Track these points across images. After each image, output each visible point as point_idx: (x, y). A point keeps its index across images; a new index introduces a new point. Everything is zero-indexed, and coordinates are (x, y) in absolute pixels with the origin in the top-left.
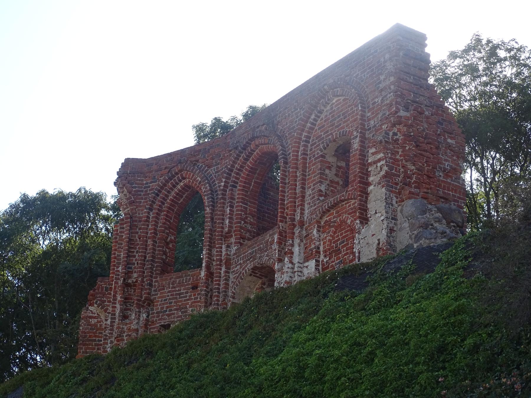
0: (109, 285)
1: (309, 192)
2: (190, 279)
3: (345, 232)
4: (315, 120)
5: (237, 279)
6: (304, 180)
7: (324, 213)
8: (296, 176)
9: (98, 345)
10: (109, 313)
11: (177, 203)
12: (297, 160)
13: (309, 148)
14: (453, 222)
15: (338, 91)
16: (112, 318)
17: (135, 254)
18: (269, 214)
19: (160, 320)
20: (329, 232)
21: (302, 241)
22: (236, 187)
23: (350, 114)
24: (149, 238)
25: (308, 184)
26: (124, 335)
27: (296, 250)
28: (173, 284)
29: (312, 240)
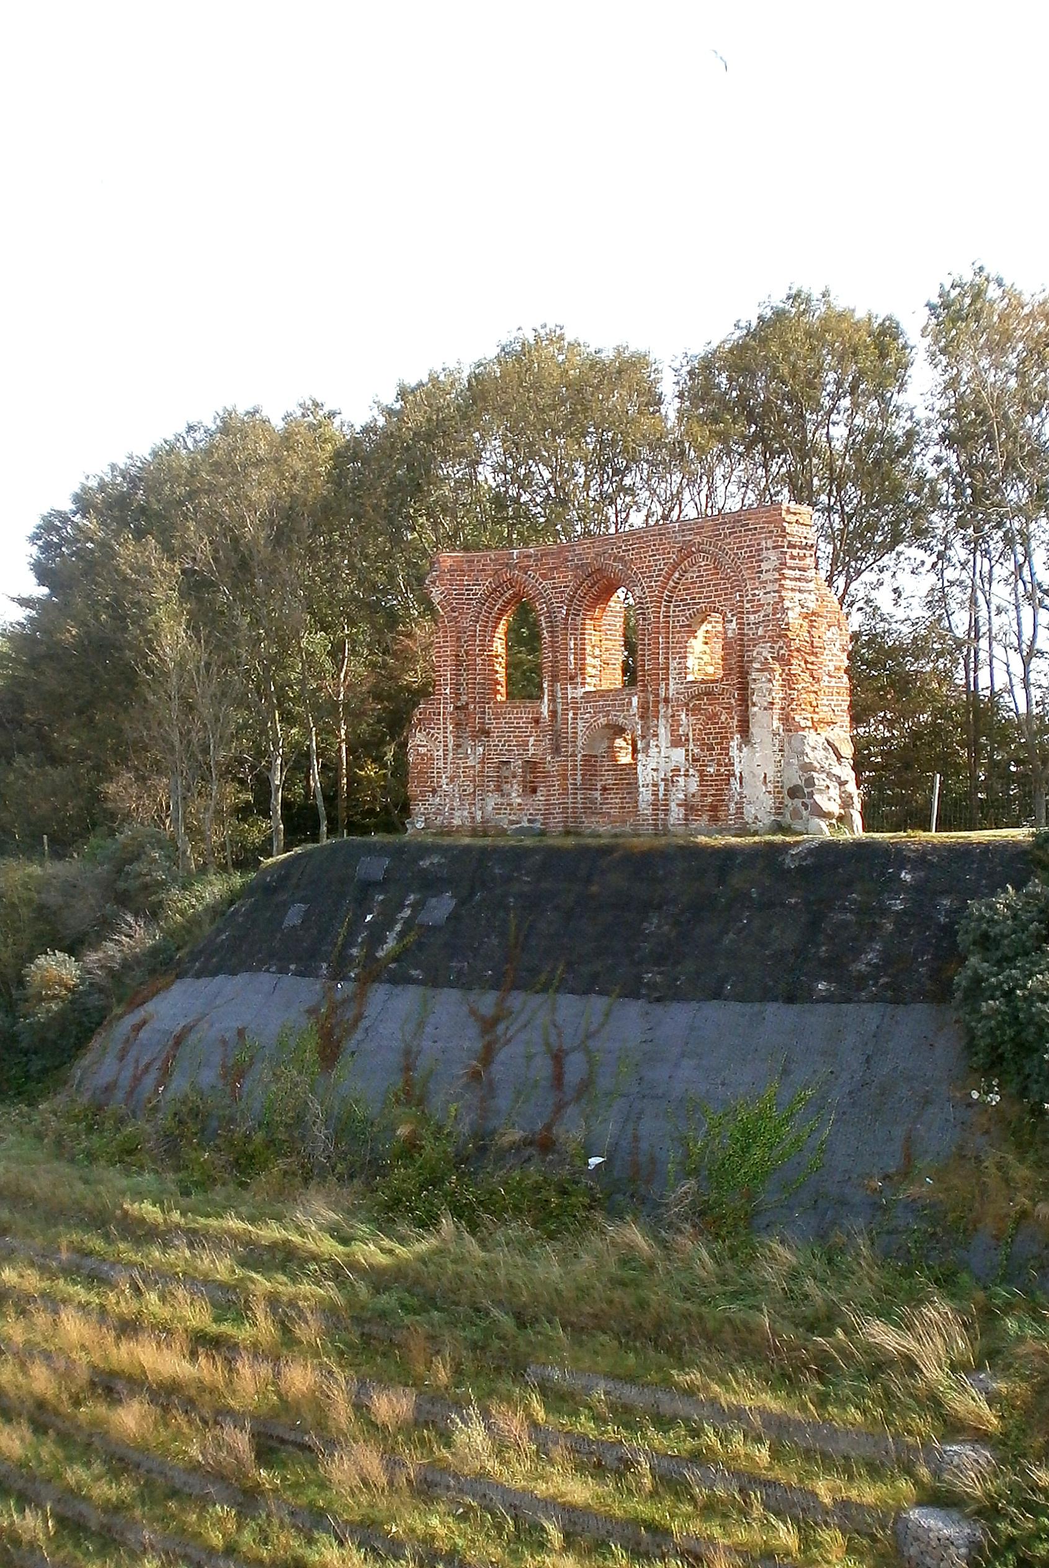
1: (673, 664)
12: (658, 622)
23: (722, 590)
27: (662, 731)
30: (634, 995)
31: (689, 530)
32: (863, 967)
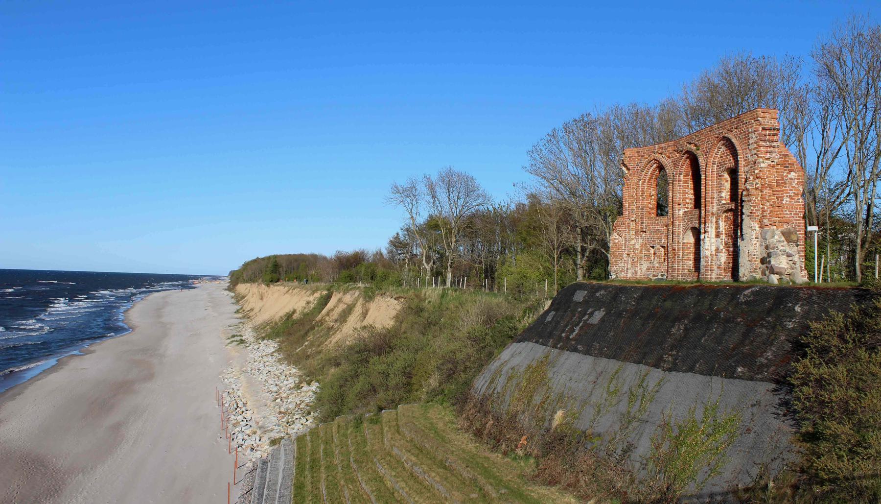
9: (620, 254)
13: (716, 168)
14: (791, 242)
16: (625, 241)
22: (682, 174)
30: (656, 366)
32: (763, 360)
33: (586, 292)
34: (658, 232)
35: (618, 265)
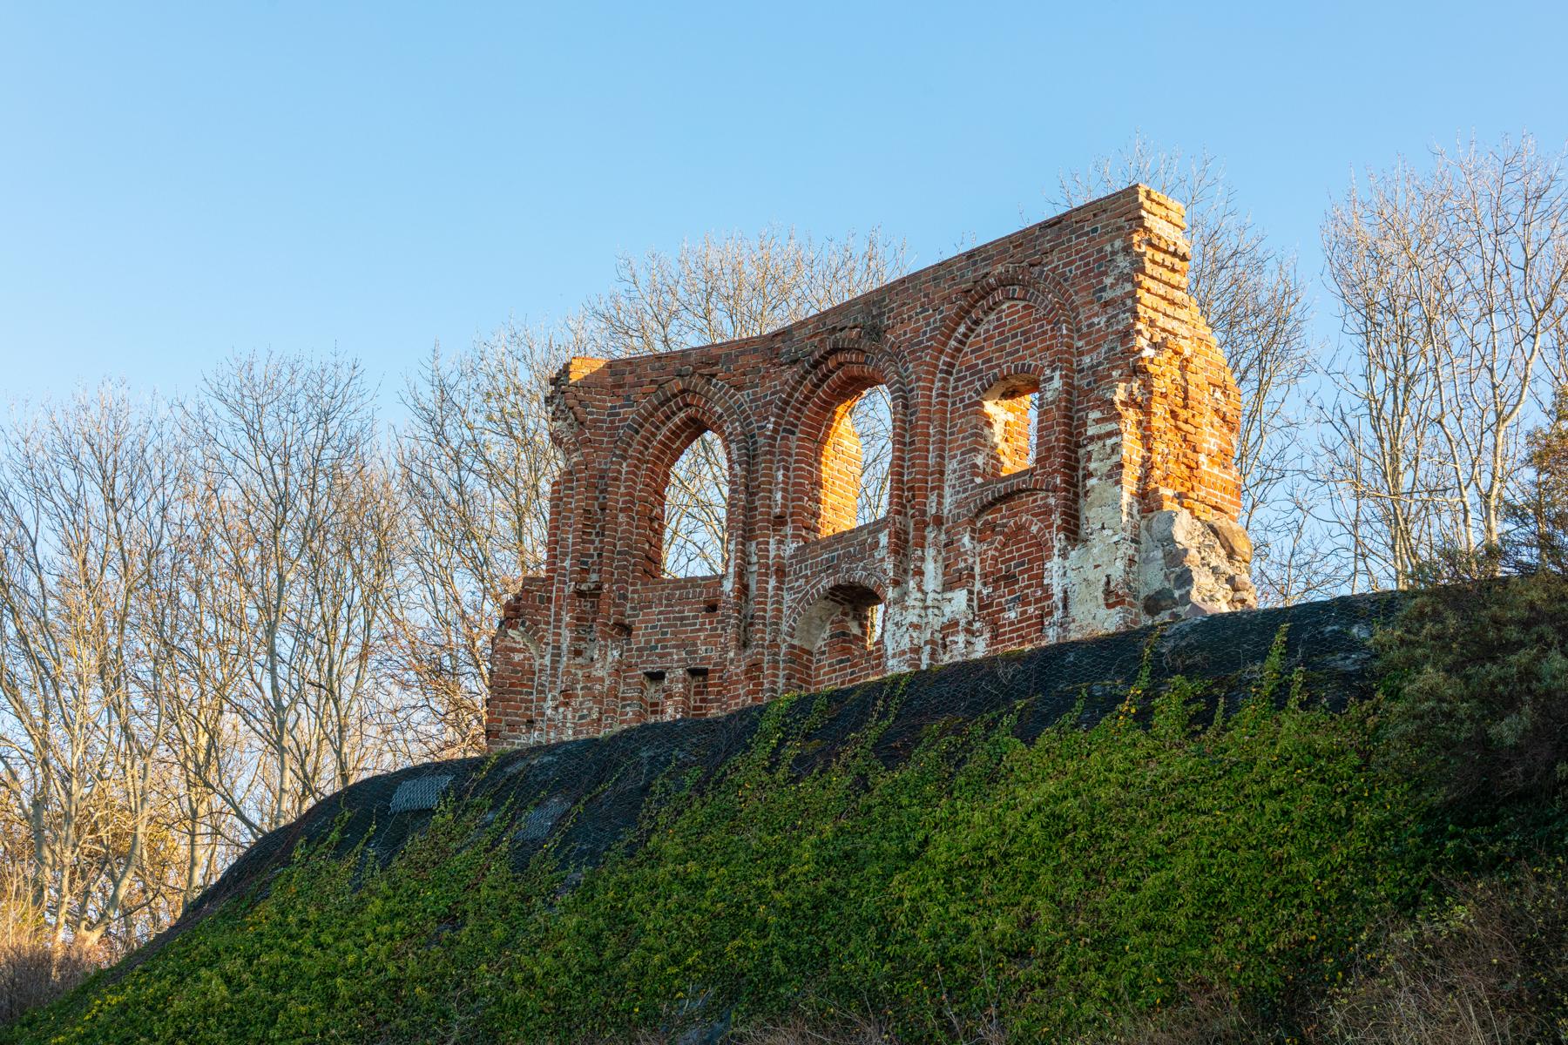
0: (546, 592)
1: (952, 466)
2: (701, 593)
3: (1026, 547)
4: (966, 336)
5: (798, 603)
6: (942, 442)
7: (984, 509)
8: (928, 435)
10: (548, 644)
11: (669, 448)
12: (930, 404)
13: (952, 384)
15: (1014, 290)
16: (553, 655)
17: (593, 537)
18: (842, 480)
19: (642, 663)
20: (992, 543)
21: (939, 552)
22: (793, 433)
24: (622, 510)
25: (950, 450)
26: (579, 687)
27: (931, 567)
28: (667, 599)
29: (960, 554)
31: (984, 260)
33: (449, 778)
34: (682, 625)
35: (516, 737)
